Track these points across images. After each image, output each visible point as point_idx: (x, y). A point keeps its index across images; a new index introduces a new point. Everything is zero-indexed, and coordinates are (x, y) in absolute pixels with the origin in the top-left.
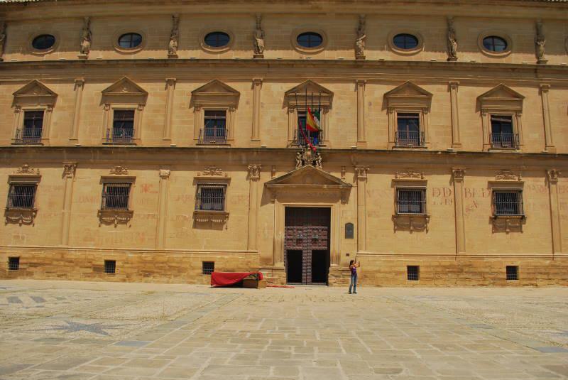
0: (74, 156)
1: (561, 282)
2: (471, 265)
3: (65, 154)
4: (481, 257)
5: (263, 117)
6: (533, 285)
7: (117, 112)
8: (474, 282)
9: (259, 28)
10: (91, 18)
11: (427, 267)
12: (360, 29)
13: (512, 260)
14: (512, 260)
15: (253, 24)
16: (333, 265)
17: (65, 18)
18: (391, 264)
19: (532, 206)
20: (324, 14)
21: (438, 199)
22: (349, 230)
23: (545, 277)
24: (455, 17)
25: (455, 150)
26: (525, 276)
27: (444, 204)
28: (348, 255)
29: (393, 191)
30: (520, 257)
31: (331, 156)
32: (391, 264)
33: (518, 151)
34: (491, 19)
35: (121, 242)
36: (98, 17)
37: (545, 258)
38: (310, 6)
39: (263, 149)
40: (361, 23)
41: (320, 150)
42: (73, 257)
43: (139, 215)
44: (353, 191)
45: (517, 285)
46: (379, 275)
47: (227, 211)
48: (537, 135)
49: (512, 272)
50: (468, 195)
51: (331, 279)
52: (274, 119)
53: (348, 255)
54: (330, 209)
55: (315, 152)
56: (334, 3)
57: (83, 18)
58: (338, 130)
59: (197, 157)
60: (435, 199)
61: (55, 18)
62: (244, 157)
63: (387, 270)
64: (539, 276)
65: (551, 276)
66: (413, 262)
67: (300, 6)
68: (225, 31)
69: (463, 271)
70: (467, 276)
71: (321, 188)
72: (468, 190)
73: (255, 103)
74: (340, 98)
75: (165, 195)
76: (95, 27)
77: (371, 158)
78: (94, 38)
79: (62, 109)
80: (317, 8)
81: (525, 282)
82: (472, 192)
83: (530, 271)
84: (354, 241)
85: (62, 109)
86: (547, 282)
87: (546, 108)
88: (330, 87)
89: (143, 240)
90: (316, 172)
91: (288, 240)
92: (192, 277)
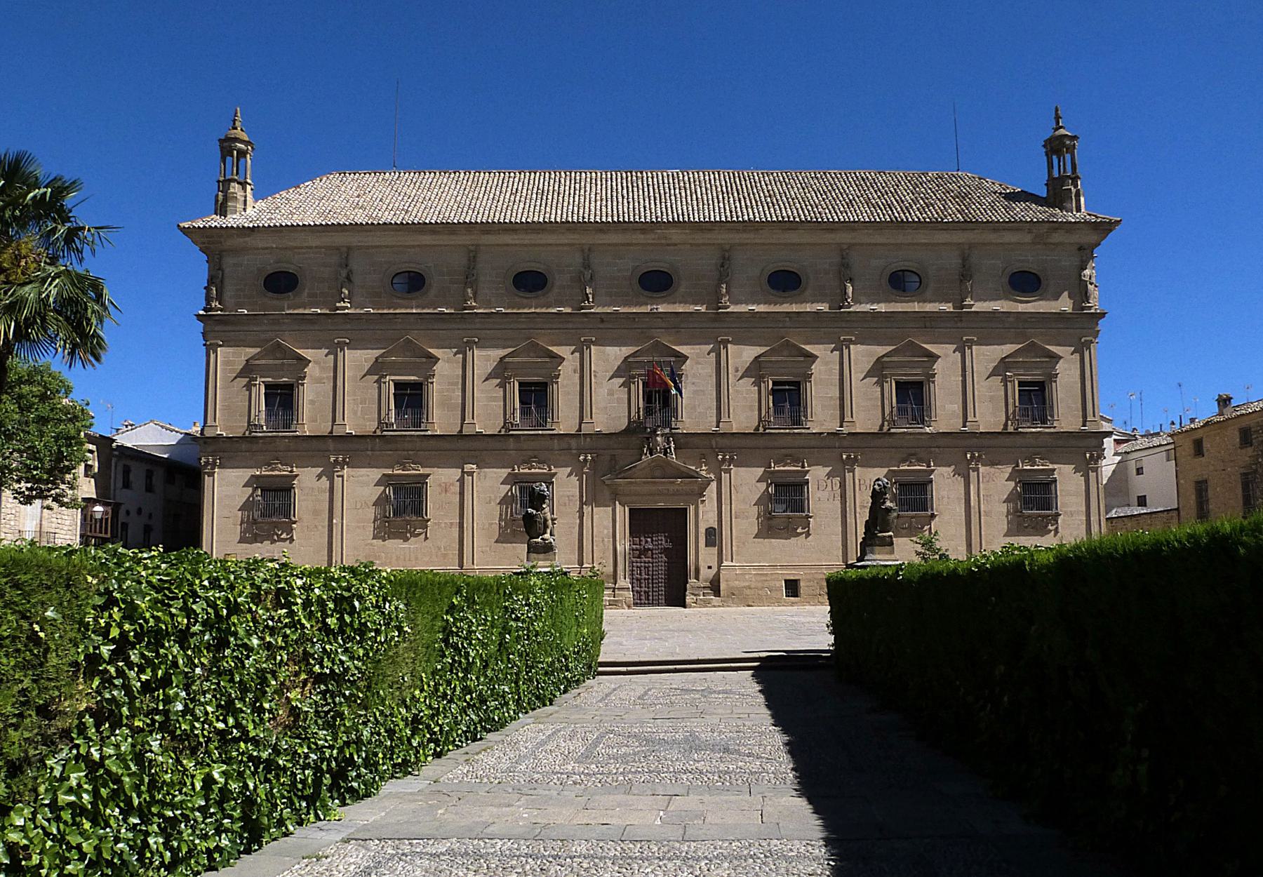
0: (336, 450)
3: (331, 445)
5: (594, 391)
7: (398, 385)
9: (587, 265)
10: (349, 248)
11: (810, 581)
12: (722, 266)
15: (578, 259)
16: (692, 581)
17: (311, 248)
19: (945, 500)
24: (851, 246)
25: (845, 430)
28: (710, 567)
31: (685, 442)
33: (928, 430)
34: (899, 246)
35: (417, 559)
36: (359, 248)
39: (599, 434)
40: (724, 258)
41: (673, 435)
43: (439, 524)
44: (714, 485)
46: (748, 592)
48: (957, 407)
50: (863, 488)
51: (689, 599)
52: (611, 393)
53: (710, 567)
54: (684, 512)
55: (666, 437)
57: (338, 249)
58: (694, 410)
59: (511, 443)
60: (819, 494)
62: (573, 443)
63: (760, 585)
68: (540, 268)
74: (698, 363)
76: (357, 264)
77: (736, 442)
78: (357, 279)
79: (319, 381)
80: (666, 238)
85: (319, 381)
88: (683, 349)
89: (445, 556)
90: (669, 464)
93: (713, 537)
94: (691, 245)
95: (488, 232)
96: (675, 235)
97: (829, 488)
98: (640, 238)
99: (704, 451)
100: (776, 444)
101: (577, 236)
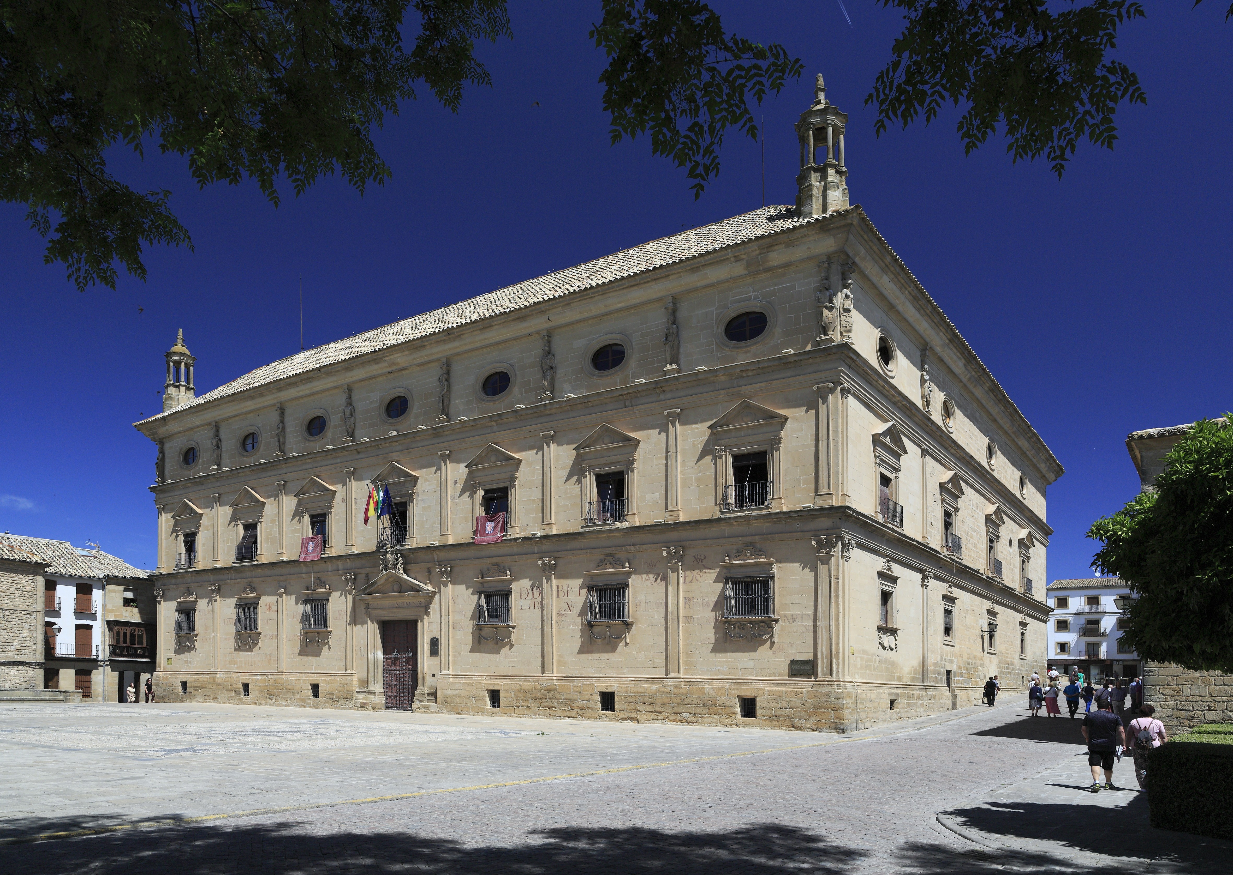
1: (673, 717)
2: (555, 689)
4: (571, 679)
6: (631, 719)
8: (559, 713)
13: (609, 684)
14: (609, 684)
18: (470, 687)
19: (643, 604)
21: (526, 603)
26: (624, 706)
27: (532, 609)
30: (620, 679)
32: (470, 687)
37: (653, 681)
38: (386, 364)
42: (221, 680)
43: (265, 636)
45: (610, 719)
47: (330, 629)
49: (608, 700)
50: (561, 594)
56: (407, 353)
61: (191, 429)
64: (642, 708)
65: (658, 708)
66: (495, 684)
67: (376, 367)
69: (548, 700)
71: (403, 596)
72: (560, 588)
73: (346, 500)
75: (280, 614)
80: (394, 364)
81: (624, 715)
82: (565, 589)
83: (630, 700)
84: (436, 659)
86: (652, 716)
87: (672, 449)
91: (387, 659)
93: (435, 646)
94: (419, 365)
95: (280, 389)
96: (401, 359)
97: (530, 596)
98: (375, 369)
99: (429, 565)
101: (334, 378)
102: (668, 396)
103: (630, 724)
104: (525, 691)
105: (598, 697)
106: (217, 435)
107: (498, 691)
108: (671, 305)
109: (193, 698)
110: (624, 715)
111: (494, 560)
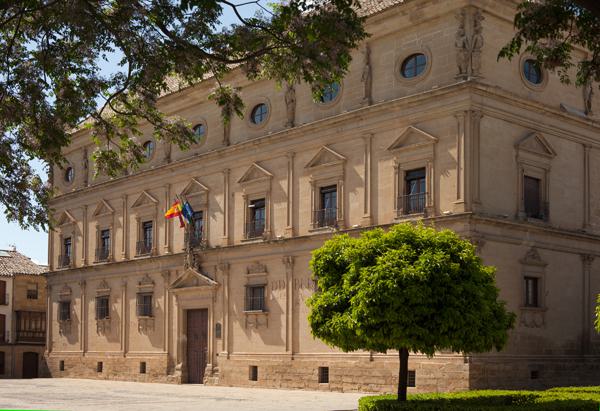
1: (364, 387)
20: (201, 103)
22: (218, 328)
23: (349, 380)
29: (244, 289)
38: (188, 100)
49: (324, 375)
70: (288, 378)
80: (195, 99)
81: (333, 386)
92: (135, 375)
93: (218, 328)
100: (249, 254)
102: (364, 123)
103: (336, 394)
104: (273, 367)
105: (317, 372)
106: (85, 157)
107: (256, 367)
108: (365, 50)
109: (67, 375)
110: (333, 386)
111: (256, 259)
